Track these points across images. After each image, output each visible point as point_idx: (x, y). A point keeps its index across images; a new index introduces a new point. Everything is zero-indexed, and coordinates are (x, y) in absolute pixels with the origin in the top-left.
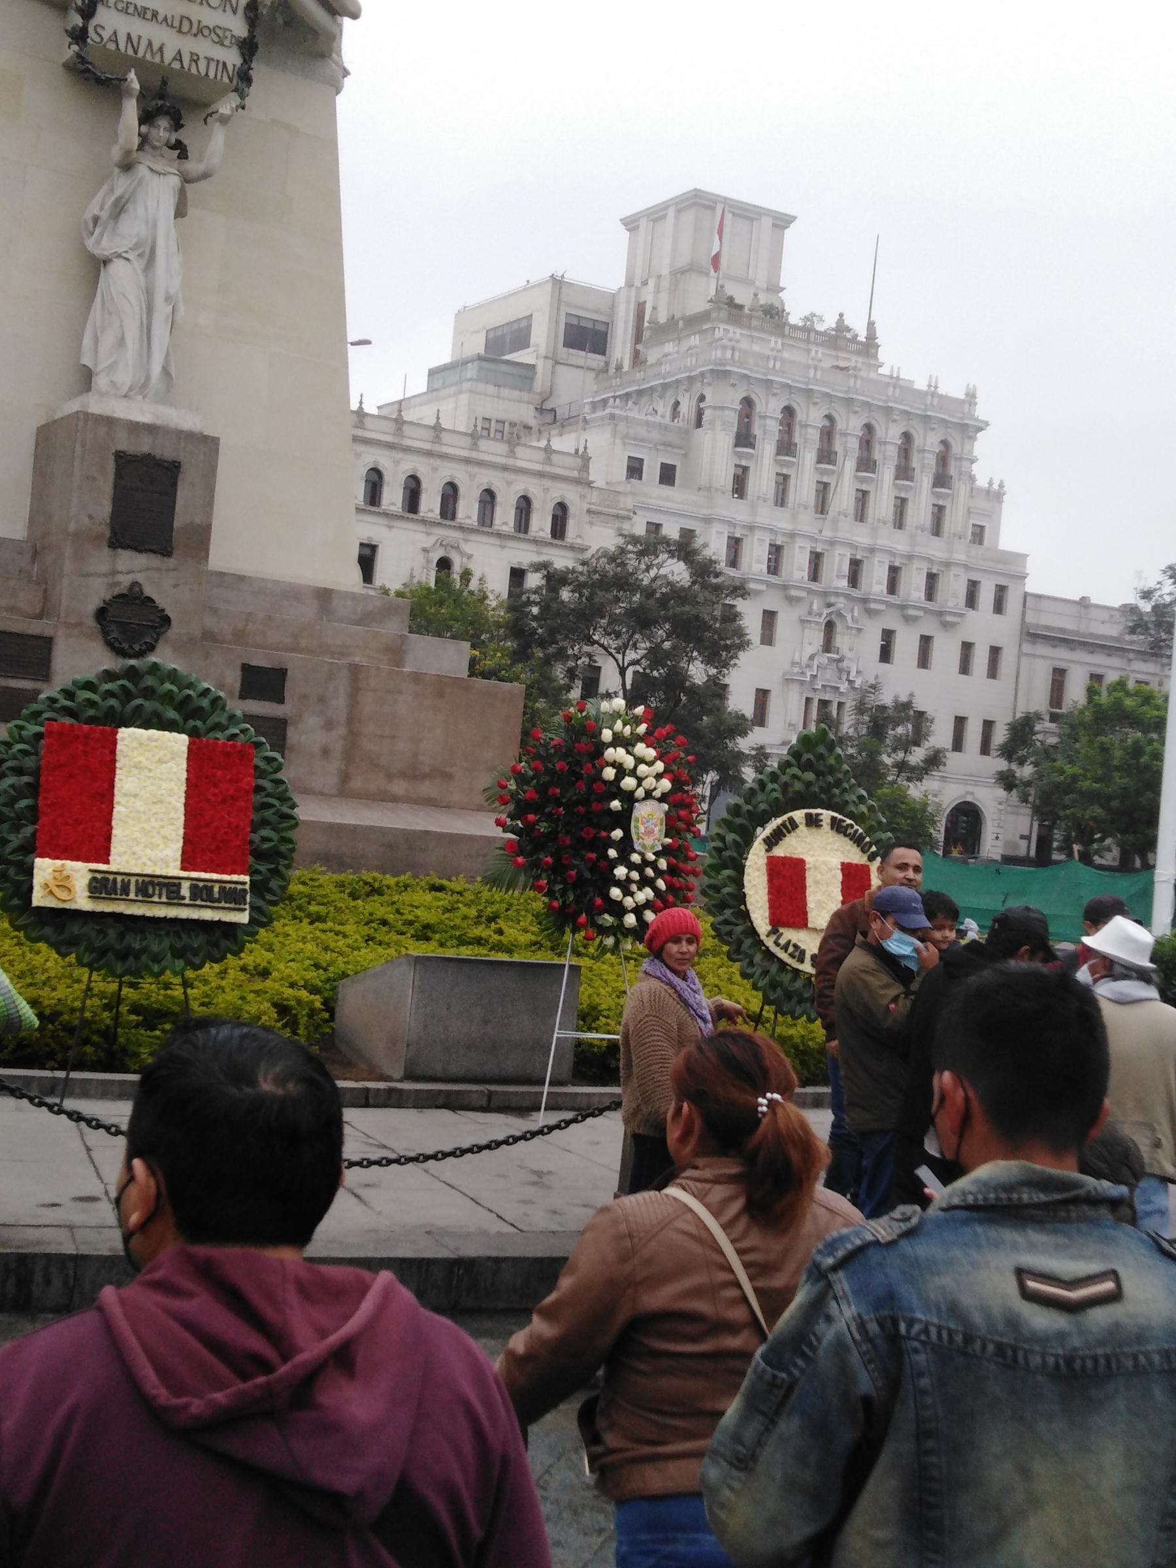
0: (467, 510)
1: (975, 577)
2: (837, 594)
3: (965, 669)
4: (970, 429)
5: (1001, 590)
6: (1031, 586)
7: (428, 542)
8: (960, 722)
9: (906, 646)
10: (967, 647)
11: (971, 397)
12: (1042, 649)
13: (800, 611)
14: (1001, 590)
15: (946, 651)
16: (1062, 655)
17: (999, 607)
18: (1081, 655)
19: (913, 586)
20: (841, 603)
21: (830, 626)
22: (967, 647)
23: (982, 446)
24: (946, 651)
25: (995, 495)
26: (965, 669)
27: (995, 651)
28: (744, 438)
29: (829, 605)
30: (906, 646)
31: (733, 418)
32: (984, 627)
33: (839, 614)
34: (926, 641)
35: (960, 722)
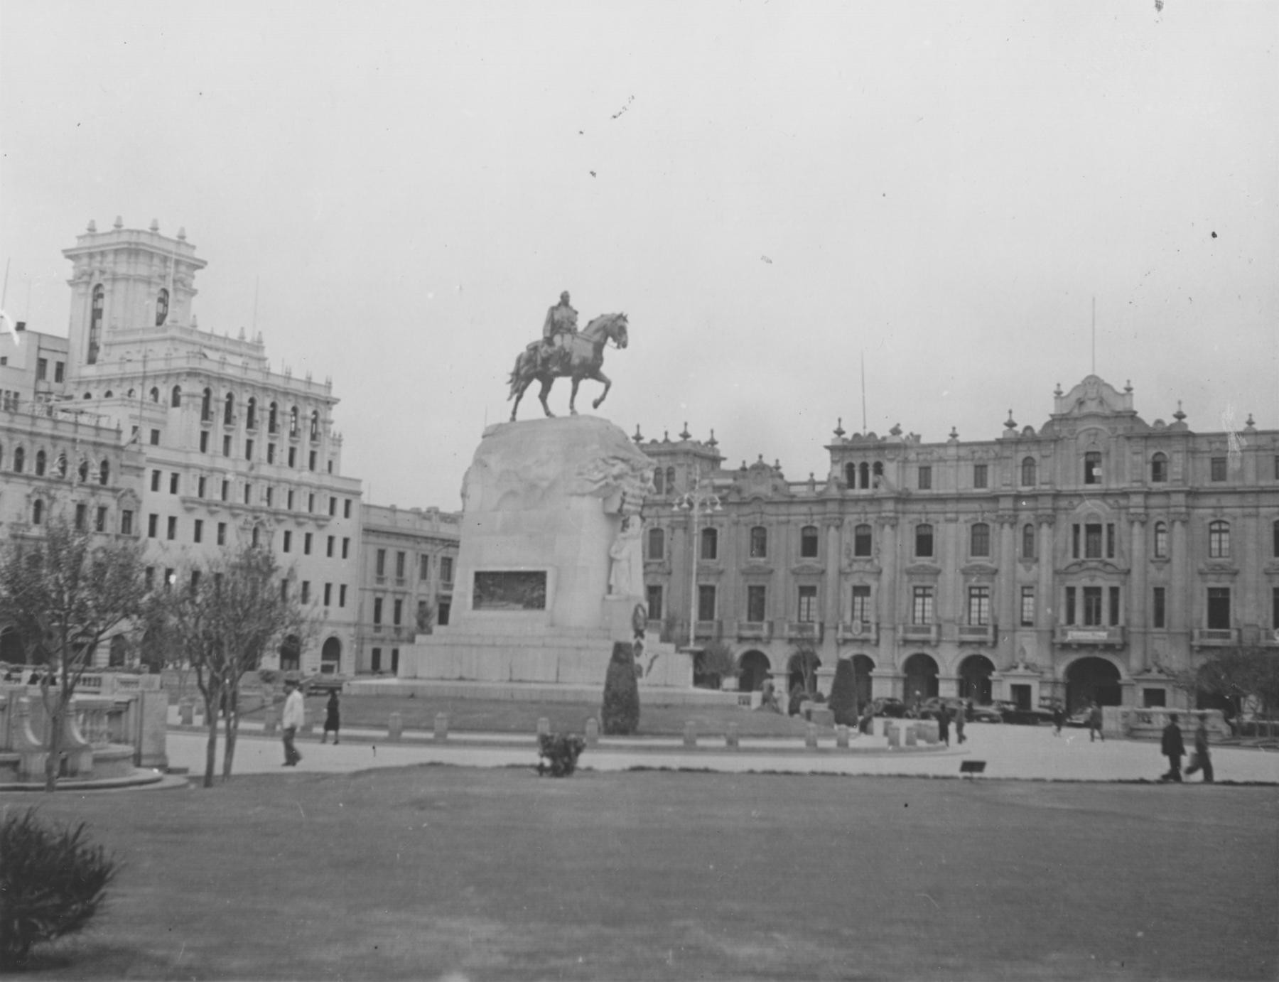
0: (52, 469)
1: (334, 495)
2: (261, 511)
3: (330, 553)
4: (329, 403)
5: (348, 503)
6: (365, 499)
7: (29, 491)
8: (328, 586)
9: (298, 542)
10: (331, 539)
11: (329, 386)
12: (372, 538)
13: (240, 522)
14: (348, 503)
15: (319, 544)
16: (383, 542)
17: (347, 515)
18: (393, 541)
19: (301, 506)
20: (264, 516)
21: (255, 531)
22: (331, 539)
23: (335, 413)
24: (319, 544)
25: (338, 441)
26: (330, 553)
27: (346, 541)
28: (206, 414)
29: (256, 518)
30: (298, 542)
31: (200, 401)
32: (341, 527)
33: (262, 523)
34: (308, 536)
35: (328, 586)
